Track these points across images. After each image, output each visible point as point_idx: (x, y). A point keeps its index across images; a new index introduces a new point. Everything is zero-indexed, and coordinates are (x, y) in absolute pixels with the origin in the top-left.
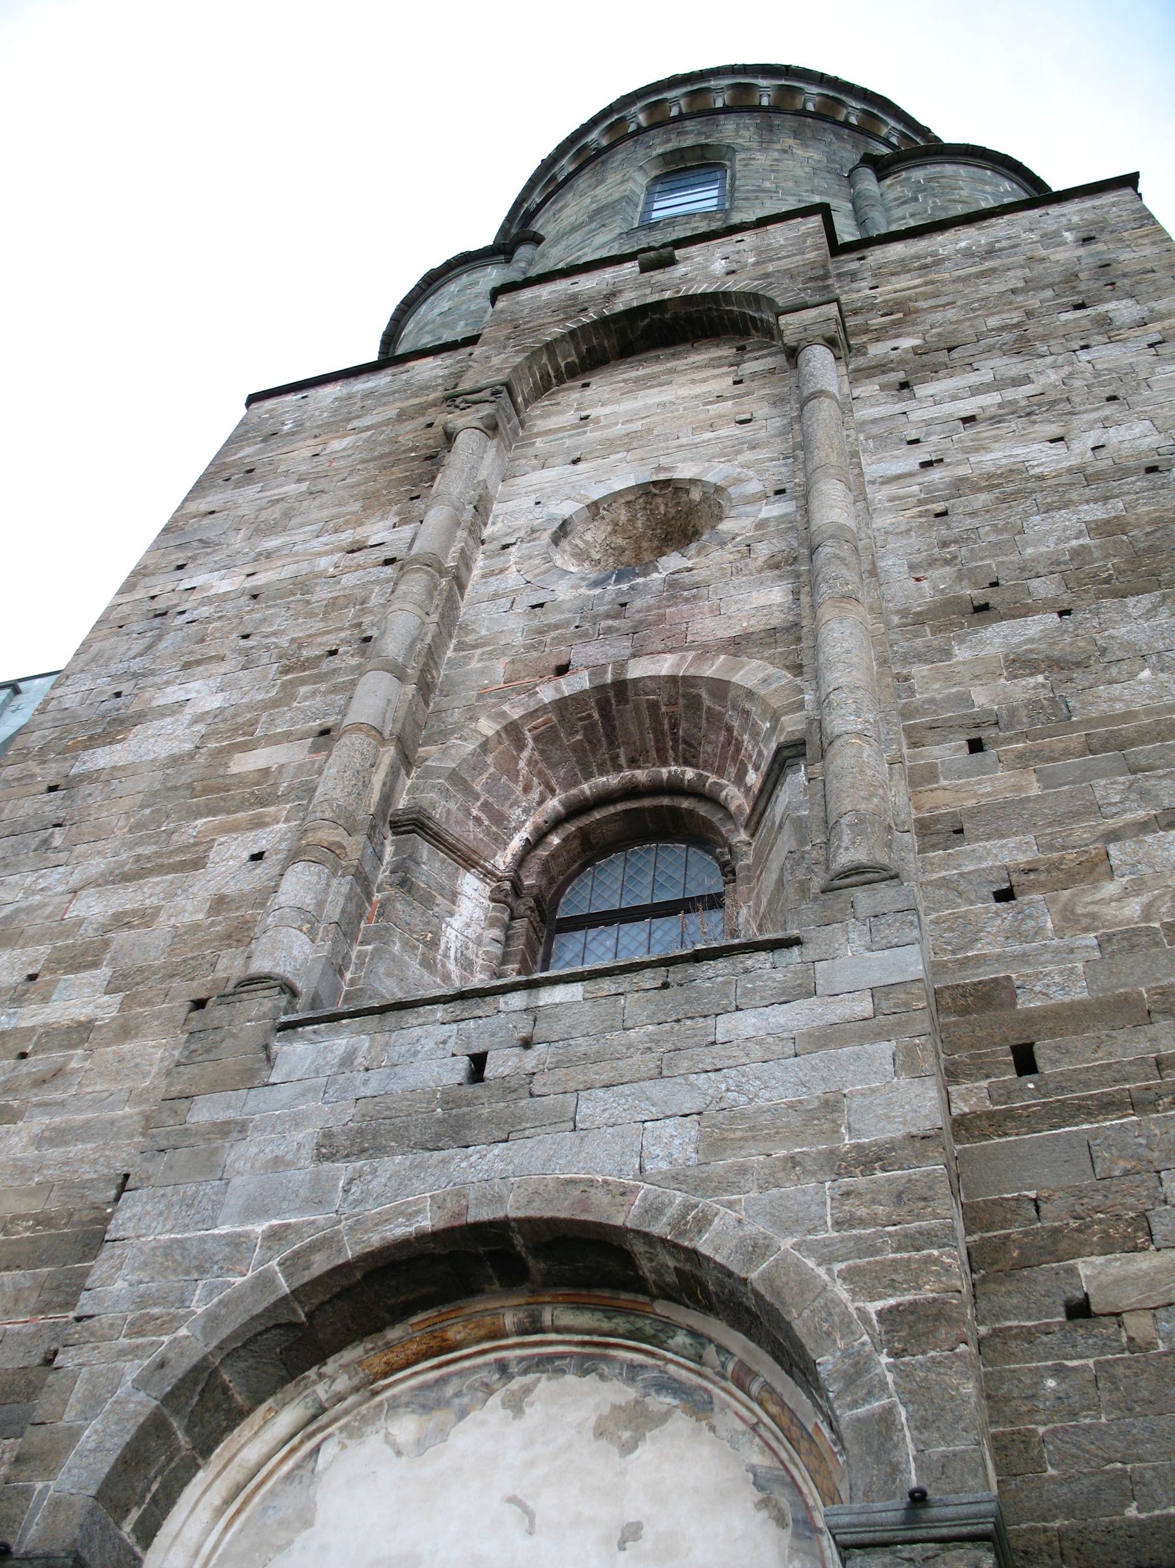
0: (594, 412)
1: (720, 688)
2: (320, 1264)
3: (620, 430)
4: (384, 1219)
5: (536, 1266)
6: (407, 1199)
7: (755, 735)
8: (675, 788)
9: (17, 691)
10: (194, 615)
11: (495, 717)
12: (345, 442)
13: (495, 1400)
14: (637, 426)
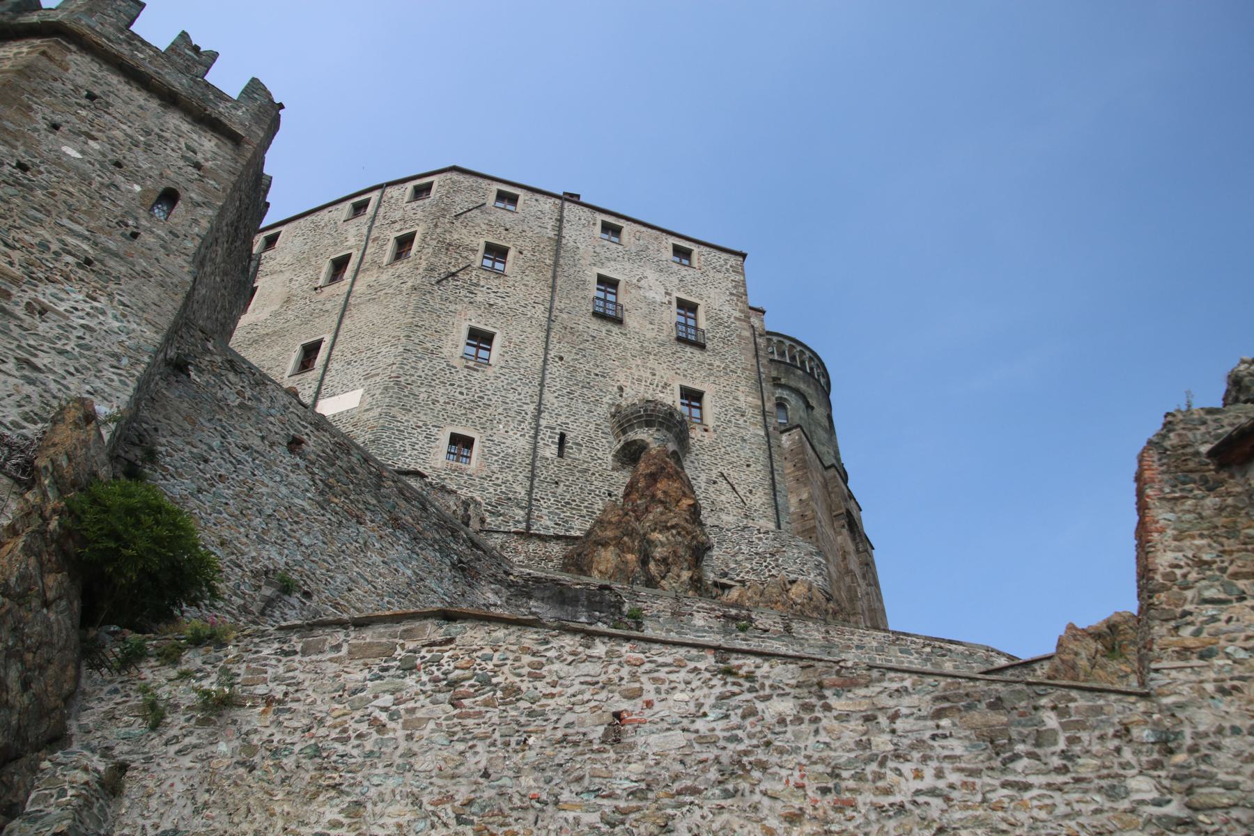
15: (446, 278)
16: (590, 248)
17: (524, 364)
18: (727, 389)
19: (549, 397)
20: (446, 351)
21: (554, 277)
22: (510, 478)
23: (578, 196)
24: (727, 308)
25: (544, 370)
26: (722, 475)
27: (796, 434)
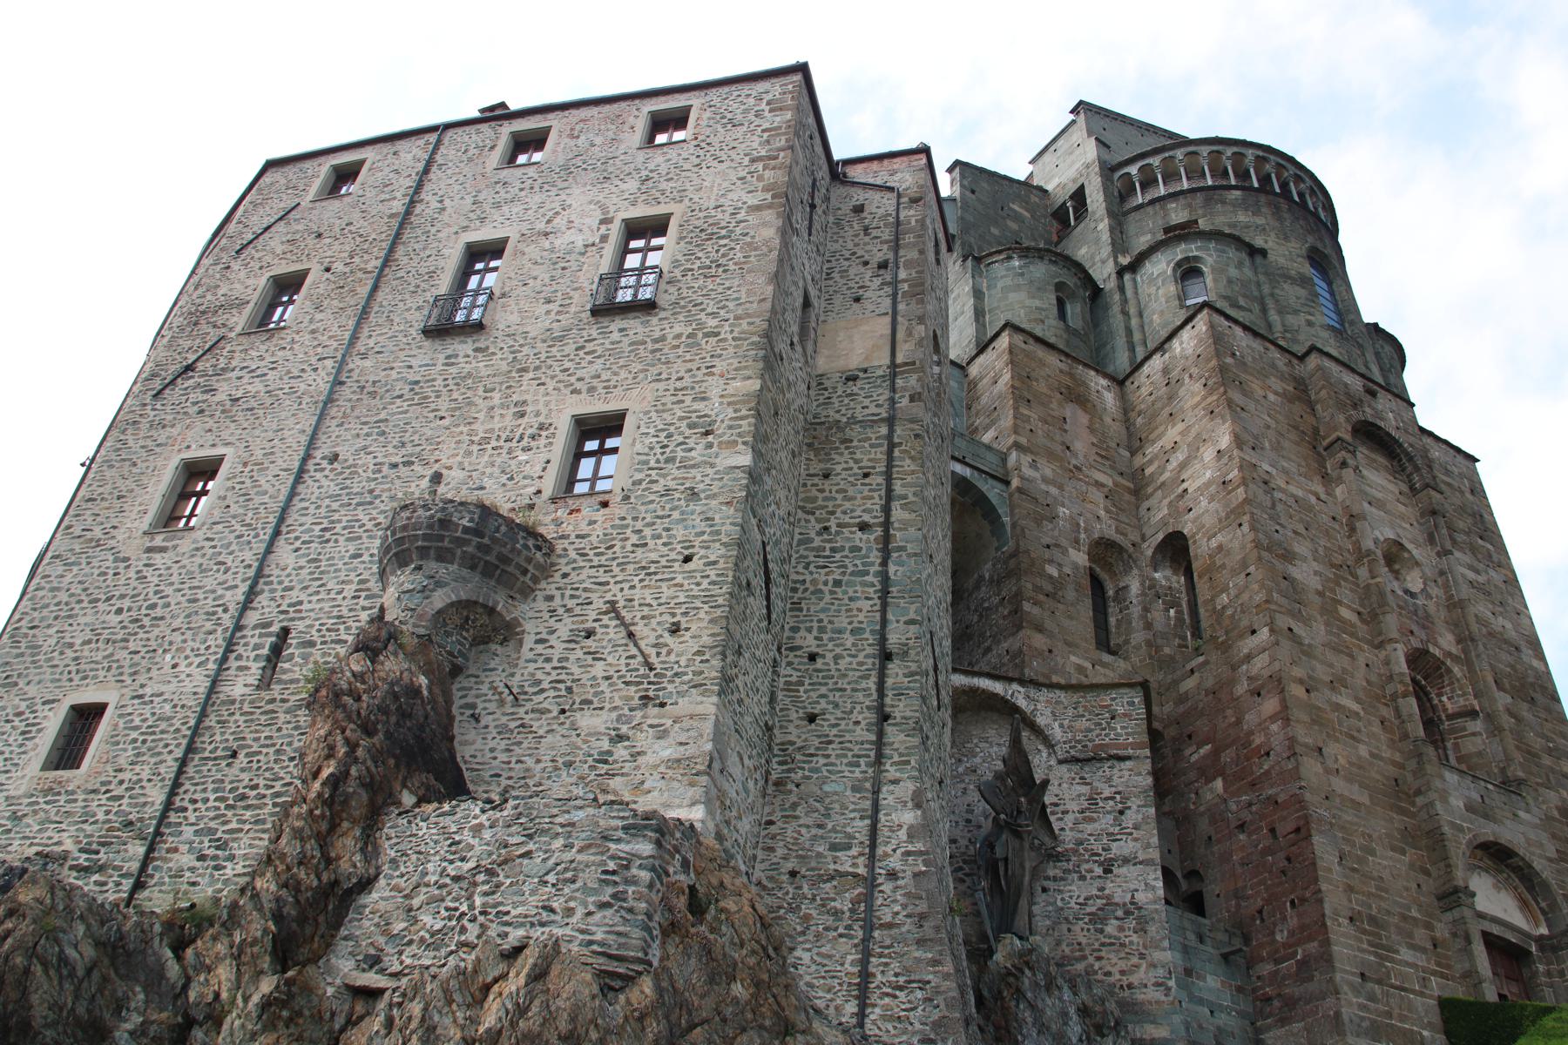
0: (1365, 472)
1: (1449, 671)
6: (1488, 831)
7: (1453, 691)
12: (1272, 397)
14: (1380, 495)
15: (173, 382)
16: (469, 200)
17: (258, 500)
18: (687, 381)
19: (284, 554)
20: (120, 535)
21: (375, 288)
22: (145, 775)
23: (503, 105)
24: (740, 195)
25: (293, 493)
26: (612, 608)
27: (1201, 323)
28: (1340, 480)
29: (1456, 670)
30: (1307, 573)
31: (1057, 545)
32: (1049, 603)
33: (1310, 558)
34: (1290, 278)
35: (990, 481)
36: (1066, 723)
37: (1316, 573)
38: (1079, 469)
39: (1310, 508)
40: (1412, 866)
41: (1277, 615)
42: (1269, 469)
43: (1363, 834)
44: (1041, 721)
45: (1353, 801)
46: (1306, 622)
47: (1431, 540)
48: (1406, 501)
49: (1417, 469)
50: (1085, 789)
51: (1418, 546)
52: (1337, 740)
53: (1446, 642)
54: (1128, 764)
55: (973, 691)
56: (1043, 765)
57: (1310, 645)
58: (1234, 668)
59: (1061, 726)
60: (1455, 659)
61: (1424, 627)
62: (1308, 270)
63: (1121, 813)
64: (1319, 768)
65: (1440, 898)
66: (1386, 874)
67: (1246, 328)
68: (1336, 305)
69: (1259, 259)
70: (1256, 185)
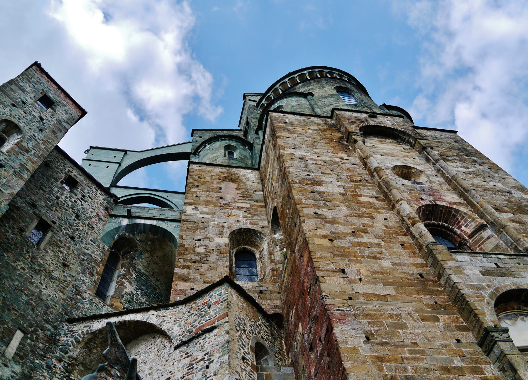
0: (376, 145)
1: (457, 211)
2: (501, 292)
3: (384, 151)
4: (505, 286)
5: (523, 298)
6: (508, 284)
7: (466, 221)
8: (443, 226)
9: (126, 154)
10: (312, 162)
11: (416, 204)
12: (311, 131)
13: (519, 319)
14: (389, 152)
28: (355, 149)
29: (462, 209)
30: (332, 186)
31: (205, 238)
32: (197, 265)
33: (334, 181)
34: (326, 97)
35: (169, 223)
36: (182, 323)
37: (339, 186)
38: (228, 205)
39: (336, 163)
40: (447, 327)
41: (304, 209)
42: (305, 154)
43: (391, 316)
44: (164, 327)
45: (376, 295)
46: (332, 208)
47: (428, 160)
48: (409, 151)
49: (409, 136)
50: (187, 361)
51: (419, 164)
52: (360, 262)
53: (450, 198)
54: (215, 332)
55: (122, 325)
56: (166, 355)
57: (333, 218)
58: (294, 252)
59: (180, 326)
60: (461, 204)
61: (430, 195)
62: (335, 92)
63: (207, 367)
64: (342, 281)
65: (481, 344)
66: (418, 340)
67: (295, 114)
68: (357, 101)
69: (309, 97)
70: (309, 78)
